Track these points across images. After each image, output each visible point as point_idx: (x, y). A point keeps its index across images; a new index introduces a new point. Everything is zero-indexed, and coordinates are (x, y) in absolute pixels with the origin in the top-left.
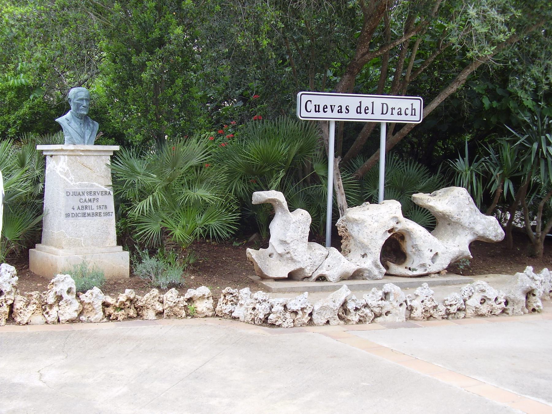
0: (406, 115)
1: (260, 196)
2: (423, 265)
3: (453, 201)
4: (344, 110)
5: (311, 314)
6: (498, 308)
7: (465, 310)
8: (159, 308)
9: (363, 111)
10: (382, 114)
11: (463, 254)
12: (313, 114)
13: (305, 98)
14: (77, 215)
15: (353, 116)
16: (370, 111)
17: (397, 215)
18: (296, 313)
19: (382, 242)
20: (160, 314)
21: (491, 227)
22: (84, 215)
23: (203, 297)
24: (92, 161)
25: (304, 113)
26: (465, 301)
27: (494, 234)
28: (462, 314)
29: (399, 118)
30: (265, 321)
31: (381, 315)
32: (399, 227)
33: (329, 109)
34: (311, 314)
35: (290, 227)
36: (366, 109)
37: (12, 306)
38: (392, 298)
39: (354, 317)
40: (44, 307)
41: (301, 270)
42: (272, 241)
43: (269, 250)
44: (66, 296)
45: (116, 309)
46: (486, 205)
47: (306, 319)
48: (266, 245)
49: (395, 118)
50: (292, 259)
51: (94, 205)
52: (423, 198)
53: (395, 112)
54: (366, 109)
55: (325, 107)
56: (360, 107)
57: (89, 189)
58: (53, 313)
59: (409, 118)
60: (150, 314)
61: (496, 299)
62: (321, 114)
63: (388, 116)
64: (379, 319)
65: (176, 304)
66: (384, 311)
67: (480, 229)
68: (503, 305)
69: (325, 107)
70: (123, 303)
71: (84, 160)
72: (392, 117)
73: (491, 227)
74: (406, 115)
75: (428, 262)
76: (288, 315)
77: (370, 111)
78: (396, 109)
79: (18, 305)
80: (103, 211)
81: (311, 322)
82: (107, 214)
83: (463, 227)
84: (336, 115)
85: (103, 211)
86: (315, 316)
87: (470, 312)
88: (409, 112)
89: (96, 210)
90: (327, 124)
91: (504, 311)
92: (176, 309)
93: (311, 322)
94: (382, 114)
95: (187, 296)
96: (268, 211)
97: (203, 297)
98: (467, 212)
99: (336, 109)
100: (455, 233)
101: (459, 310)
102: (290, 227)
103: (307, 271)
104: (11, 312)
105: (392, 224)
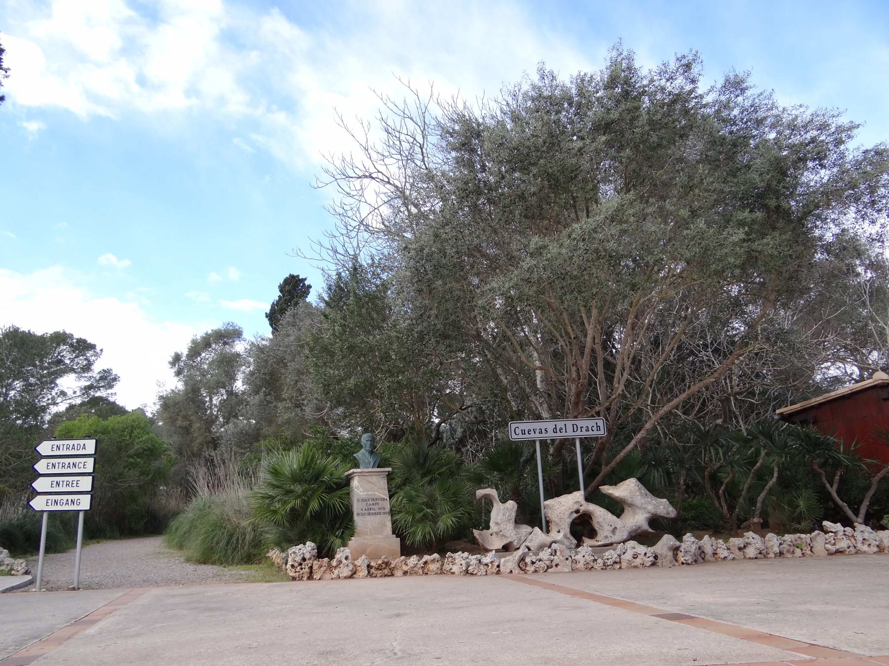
1: (480, 493)
2: (606, 537)
3: (627, 489)
4: (543, 431)
5: (498, 566)
6: (649, 561)
7: (620, 562)
8: (405, 568)
11: (639, 528)
12: (521, 436)
13: (513, 426)
14: (365, 514)
15: (551, 434)
16: (564, 430)
18: (487, 565)
19: (569, 520)
20: (405, 573)
21: (663, 507)
22: (369, 514)
23: (433, 561)
24: (374, 479)
25: (514, 436)
26: (620, 556)
27: (665, 512)
28: (618, 566)
29: (588, 433)
30: (467, 572)
31: (552, 567)
32: (582, 509)
33: (532, 432)
34: (498, 566)
35: (503, 513)
36: (561, 429)
37: (311, 568)
38: (558, 553)
39: (531, 568)
40: (330, 567)
41: (511, 543)
42: (492, 524)
43: (490, 531)
44: (344, 561)
45: (377, 569)
46: (654, 491)
47: (495, 570)
48: (488, 528)
49: (584, 434)
50: (503, 535)
51: (376, 507)
52: (607, 489)
54: (561, 429)
55: (529, 431)
57: (372, 497)
58: (336, 572)
59: (595, 432)
60: (398, 573)
61: (645, 554)
62: (527, 436)
63: (579, 433)
64: (550, 570)
65: (416, 565)
66: (554, 564)
67: (650, 508)
68: (651, 559)
69: (529, 431)
70: (380, 565)
71: (369, 478)
72: (582, 433)
73: (663, 507)
75: (609, 534)
76: (482, 567)
77: (564, 430)
79: (315, 567)
80: (382, 511)
81: (498, 572)
82: (385, 513)
83: (640, 508)
84: (538, 435)
85: (382, 511)
86: (502, 568)
87: (624, 564)
89: (377, 511)
90: (534, 441)
91: (653, 564)
92: (415, 569)
93: (498, 572)
95: (424, 560)
96: (488, 502)
97: (433, 561)
99: (537, 432)
100: (634, 514)
101: (615, 562)
102: (503, 513)
103: (515, 543)
104: (311, 572)
105: (576, 507)
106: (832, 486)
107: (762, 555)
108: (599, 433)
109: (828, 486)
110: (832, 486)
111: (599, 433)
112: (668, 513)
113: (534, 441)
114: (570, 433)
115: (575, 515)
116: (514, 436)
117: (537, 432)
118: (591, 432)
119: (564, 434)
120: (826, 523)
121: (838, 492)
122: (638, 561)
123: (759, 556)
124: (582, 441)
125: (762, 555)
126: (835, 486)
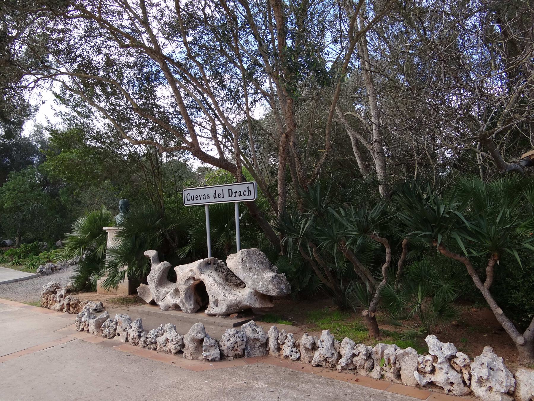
0: (245, 195)
4: (207, 197)
9: (217, 196)
10: (229, 197)
11: (240, 303)
16: (221, 196)
17: (193, 269)
28: (153, 347)
29: (240, 198)
33: (199, 198)
36: (220, 194)
53: (237, 194)
54: (220, 194)
56: (215, 194)
69: (197, 197)
74: (245, 195)
77: (221, 196)
78: (238, 192)
88: (246, 193)
94: (229, 197)
98: (240, 269)
99: (202, 197)
105: (190, 274)
106: (483, 281)
107: (329, 364)
108: (250, 197)
109: (476, 279)
110: (483, 281)
111: (250, 197)
112: (268, 291)
113: (233, 204)
114: (226, 199)
115: (192, 282)
116: (187, 202)
117: (202, 197)
118: (243, 197)
119: (221, 199)
120: (431, 340)
121: (491, 290)
122: (167, 348)
123: (324, 364)
124: (242, 206)
125: (329, 364)
126: (488, 283)
